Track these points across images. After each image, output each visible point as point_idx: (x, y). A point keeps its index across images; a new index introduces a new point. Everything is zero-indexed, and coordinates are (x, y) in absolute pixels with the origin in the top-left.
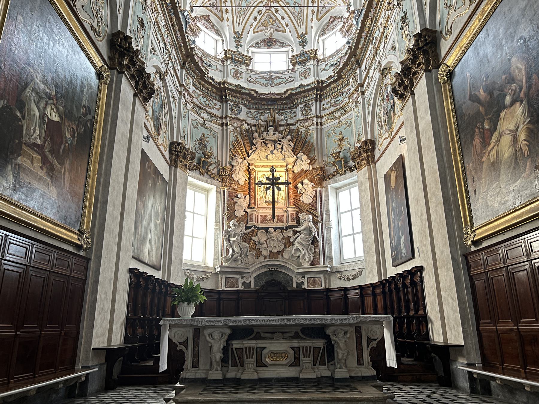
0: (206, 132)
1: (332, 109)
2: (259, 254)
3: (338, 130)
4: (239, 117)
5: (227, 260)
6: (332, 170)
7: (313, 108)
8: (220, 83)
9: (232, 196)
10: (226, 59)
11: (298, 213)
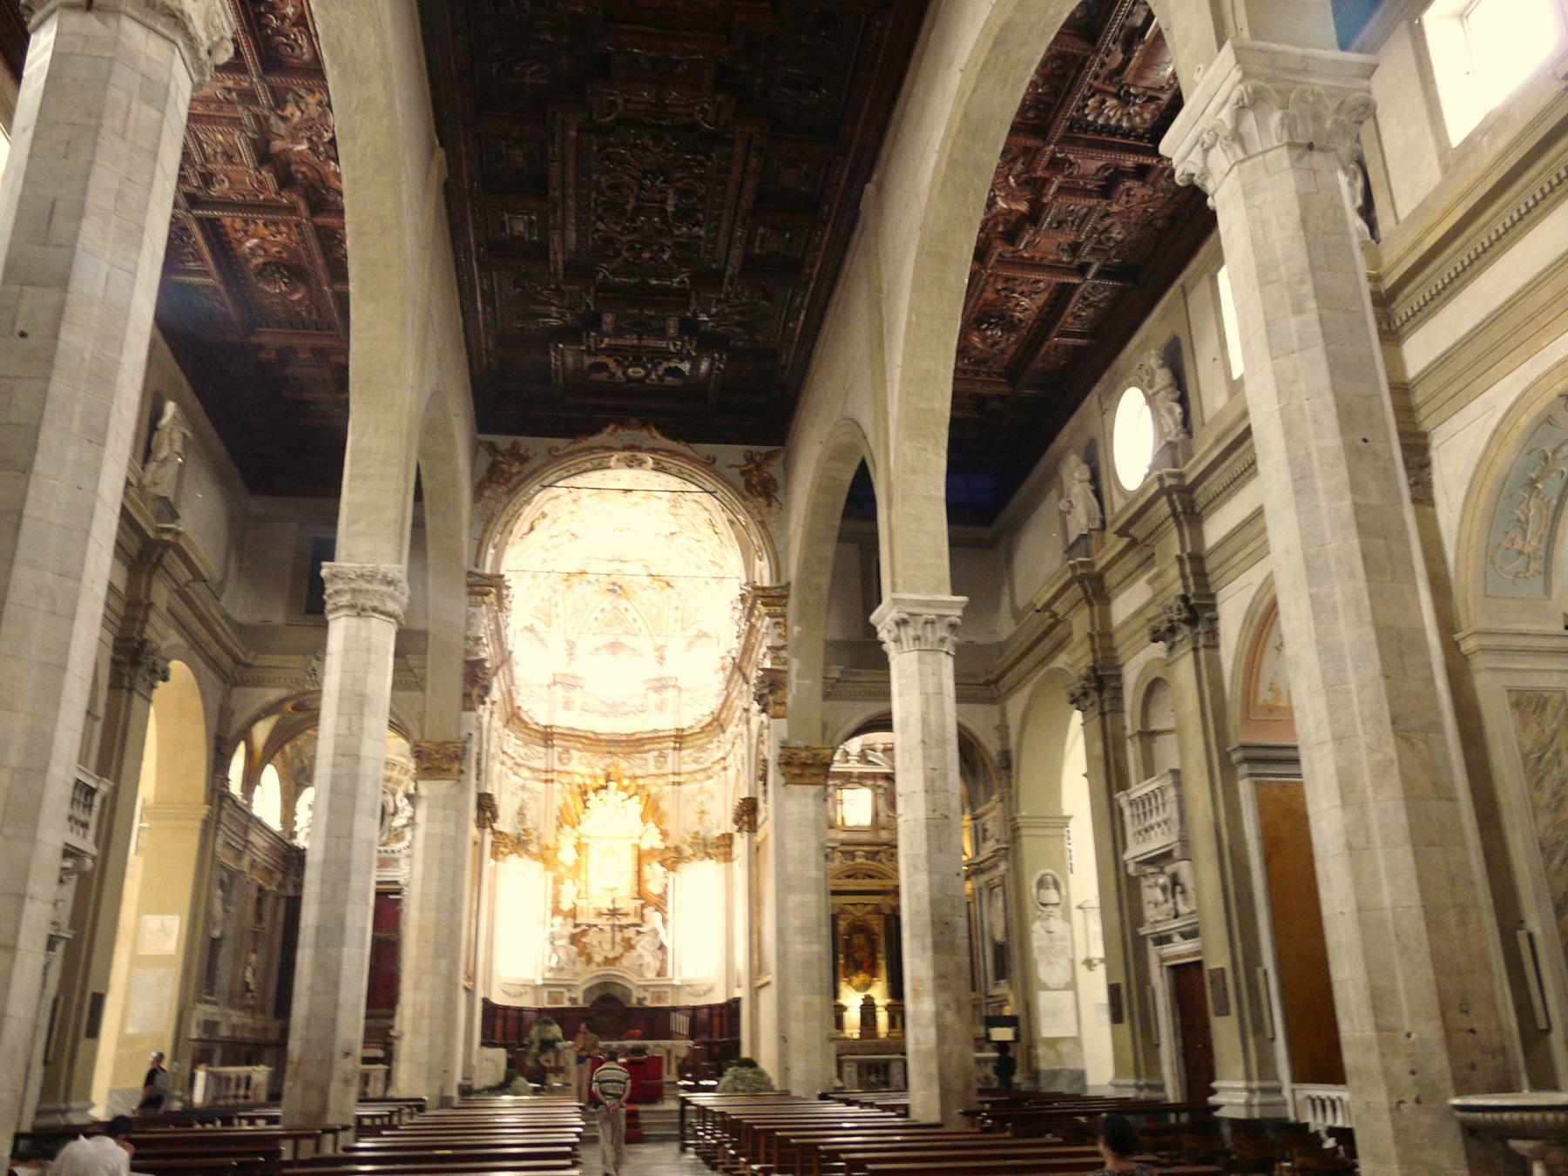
0: (526, 795)
1: (694, 767)
2: (589, 960)
3: (699, 798)
4: (568, 768)
5: (551, 969)
6: (688, 851)
7: (670, 759)
8: (545, 727)
9: (558, 881)
10: (555, 683)
11: (643, 907)
